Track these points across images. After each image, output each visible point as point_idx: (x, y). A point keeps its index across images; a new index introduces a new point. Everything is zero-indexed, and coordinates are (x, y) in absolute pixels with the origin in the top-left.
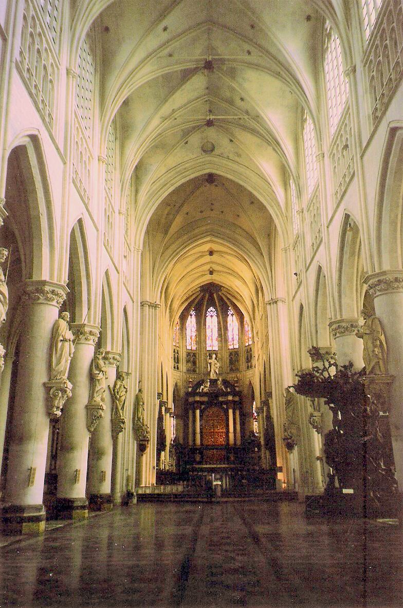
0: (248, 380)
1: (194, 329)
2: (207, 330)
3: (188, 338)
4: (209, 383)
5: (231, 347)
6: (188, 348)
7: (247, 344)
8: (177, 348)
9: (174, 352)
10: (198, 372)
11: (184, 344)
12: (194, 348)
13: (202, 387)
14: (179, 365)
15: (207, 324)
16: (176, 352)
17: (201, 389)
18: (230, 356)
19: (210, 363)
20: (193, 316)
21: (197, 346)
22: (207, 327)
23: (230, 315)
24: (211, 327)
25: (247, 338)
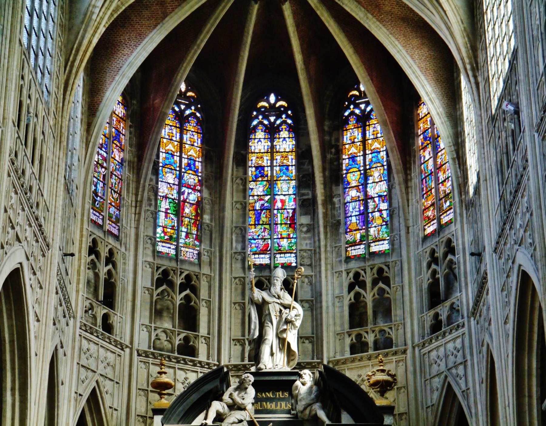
0: (437, 382)
1: (190, 178)
2: (252, 185)
3: (164, 205)
4: (251, 392)
5: (360, 250)
6: (161, 248)
7: (430, 229)
8: (111, 240)
9: (93, 250)
10: (202, 357)
11: (145, 231)
12: (189, 254)
13: (216, 406)
14: (115, 320)
15: (253, 160)
16: (104, 253)
17: (212, 414)
18: (351, 287)
19: (262, 307)
20: (191, 126)
21: (205, 246)
22: (251, 171)
23: (352, 121)
24: (268, 170)
25: (430, 202)
